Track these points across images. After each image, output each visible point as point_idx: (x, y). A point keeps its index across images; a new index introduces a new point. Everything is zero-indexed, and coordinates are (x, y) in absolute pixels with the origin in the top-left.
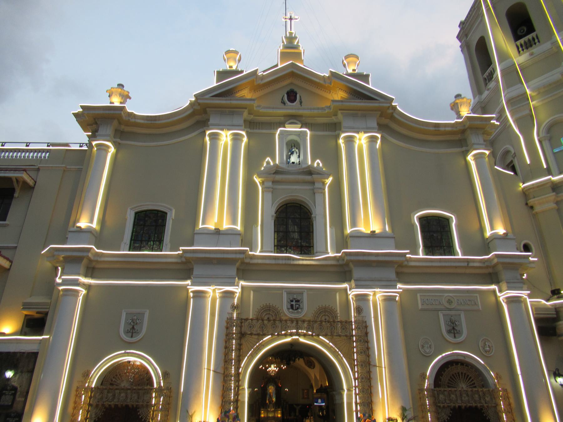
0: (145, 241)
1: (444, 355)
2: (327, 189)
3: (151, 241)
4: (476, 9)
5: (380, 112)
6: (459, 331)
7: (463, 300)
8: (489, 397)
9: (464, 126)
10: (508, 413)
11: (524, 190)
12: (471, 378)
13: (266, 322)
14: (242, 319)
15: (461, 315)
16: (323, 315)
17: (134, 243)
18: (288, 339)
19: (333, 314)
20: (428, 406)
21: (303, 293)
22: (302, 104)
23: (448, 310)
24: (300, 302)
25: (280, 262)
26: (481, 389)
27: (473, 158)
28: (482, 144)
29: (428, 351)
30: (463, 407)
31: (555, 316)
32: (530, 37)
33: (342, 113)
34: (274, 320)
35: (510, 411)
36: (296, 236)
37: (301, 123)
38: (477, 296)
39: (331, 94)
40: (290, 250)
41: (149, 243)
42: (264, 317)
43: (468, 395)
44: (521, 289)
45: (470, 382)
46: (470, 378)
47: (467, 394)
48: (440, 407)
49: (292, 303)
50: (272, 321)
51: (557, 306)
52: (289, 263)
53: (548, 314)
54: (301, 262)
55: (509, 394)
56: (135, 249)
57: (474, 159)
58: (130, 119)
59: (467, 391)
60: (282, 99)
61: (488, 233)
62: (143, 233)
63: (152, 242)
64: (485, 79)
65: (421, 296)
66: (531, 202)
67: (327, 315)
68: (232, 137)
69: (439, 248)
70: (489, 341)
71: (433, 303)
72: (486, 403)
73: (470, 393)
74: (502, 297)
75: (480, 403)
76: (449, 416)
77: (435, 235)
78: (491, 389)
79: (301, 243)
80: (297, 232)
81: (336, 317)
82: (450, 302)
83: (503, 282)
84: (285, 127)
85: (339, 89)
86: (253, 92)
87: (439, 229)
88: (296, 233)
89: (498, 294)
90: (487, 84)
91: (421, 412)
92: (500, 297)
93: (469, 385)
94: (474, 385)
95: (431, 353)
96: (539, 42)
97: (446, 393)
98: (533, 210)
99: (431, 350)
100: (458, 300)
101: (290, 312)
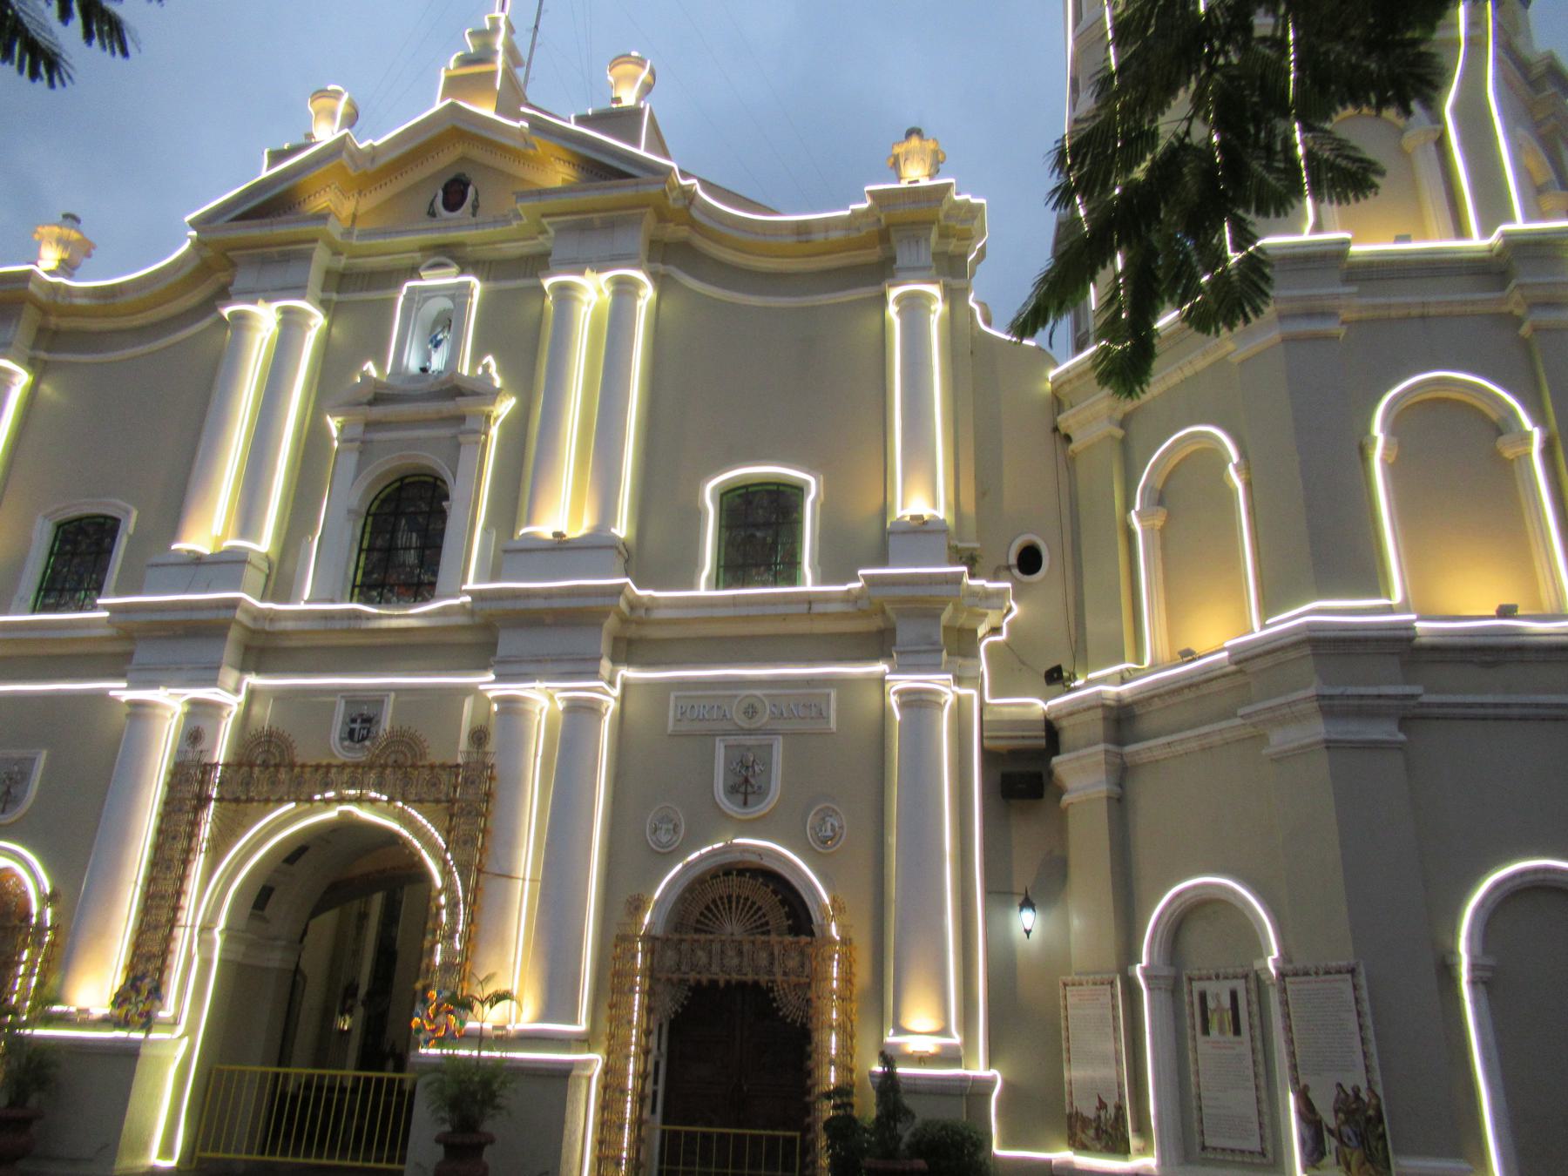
0: (70, 590)
1: (704, 851)
2: (494, 432)
3: (81, 590)
6: (760, 787)
8: (797, 959)
13: (256, 770)
14: (206, 765)
15: (775, 747)
16: (392, 752)
17: (45, 597)
18: (332, 814)
19: (416, 749)
21: (383, 702)
22: (479, 211)
23: (744, 735)
24: (374, 722)
25: (338, 625)
30: (722, 983)
34: (277, 766)
36: (411, 557)
37: (457, 263)
40: (390, 595)
41: (77, 595)
42: (256, 758)
44: (935, 668)
46: (760, 908)
48: (659, 980)
49: (353, 726)
50: (272, 769)
51: (1052, 716)
52: (357, 627)
53: (1016, 738)
54: (385, 624)
56: (46, 608)
58: (59, 299)
59: (740, 942)
60: (432, 204)
62: (69, 571)
63: (83, 593)
65: (677, 697)
66: (1066, 421)
67: (402, 752)
68: (280, 317)
69: (762, 569)
70: (837, 813)
71: (706, 716)
72: (785, 974)
73: (746, 947)
75: (770, 972)
76: (682, 1005)
77: (759, 534)
79: (419, 575)
80: (416, 548)
81: (421, 755)
82: (751, 711)
84: (420, 278)
86: (356, 195)
88: (412, 552)
93: (752, 929)
94: (765, 929)
95: (673, 847)
97: (684, 946)
100: (774, 705)
101: (343, 748)
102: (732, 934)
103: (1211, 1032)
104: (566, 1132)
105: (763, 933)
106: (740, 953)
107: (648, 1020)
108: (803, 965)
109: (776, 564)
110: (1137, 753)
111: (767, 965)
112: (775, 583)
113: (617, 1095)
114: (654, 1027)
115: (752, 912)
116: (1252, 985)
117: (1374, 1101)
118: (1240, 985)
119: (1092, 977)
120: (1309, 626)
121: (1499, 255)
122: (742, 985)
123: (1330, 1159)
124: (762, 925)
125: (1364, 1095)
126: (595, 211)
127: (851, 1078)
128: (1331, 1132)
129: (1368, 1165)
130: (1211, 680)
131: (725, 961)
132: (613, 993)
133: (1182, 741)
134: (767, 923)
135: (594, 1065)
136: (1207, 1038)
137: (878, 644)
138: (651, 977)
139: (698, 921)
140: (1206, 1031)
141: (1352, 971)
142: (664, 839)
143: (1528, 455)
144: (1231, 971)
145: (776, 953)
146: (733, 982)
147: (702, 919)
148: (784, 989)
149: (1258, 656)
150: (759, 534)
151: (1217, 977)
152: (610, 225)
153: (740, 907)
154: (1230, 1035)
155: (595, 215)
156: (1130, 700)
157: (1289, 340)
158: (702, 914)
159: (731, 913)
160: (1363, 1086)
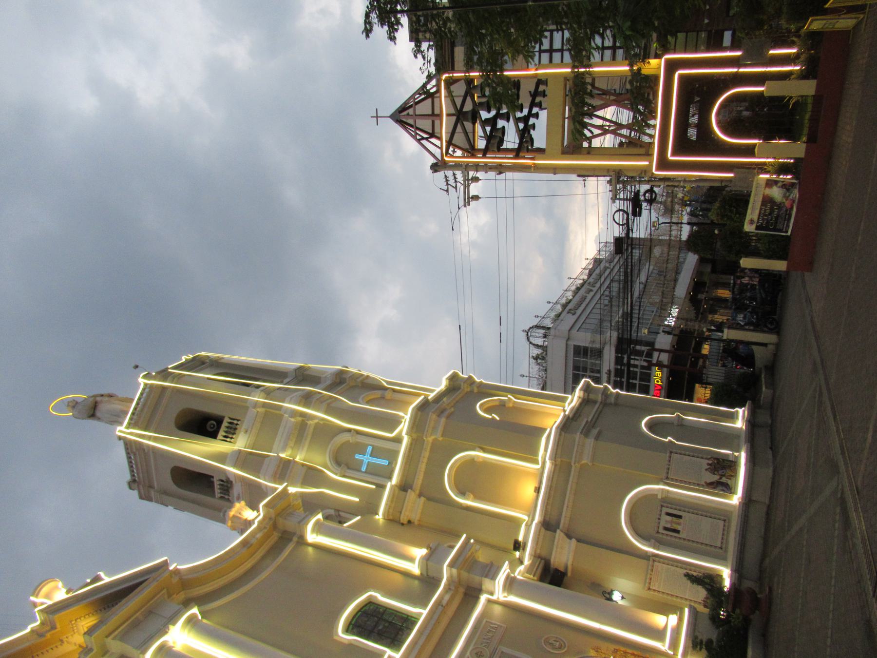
4: (137, 453)
5: (165, 590)
7: (484, 639)
9: (270, 519)
11: (386, 518)
15: (504, 651)
27: (314, 535)
28: (307, 516)
31: (543, 561)
32: (225, 424)
33: (113, 639)
38: (487, 622)
39: (65, 642)
51: (533, 553)
53: (538, 566)
57: (317, 535)
61: (415, 569)
64: (221, 497)
66: (404, 519)
69: (400, 633)
74: (500, 595)
77: (380, 628)
83: (483, 582)
85: (76, 620)
87: (376, 619)
89: (494, 598)
90: (228, 499)
92: (498, 598)
96: (238, 420)
98: (414, 523)
100: (482, 644)
103: (679, 529)
109: (402, 626)
110: (564, 523)
112: (411, 630)
116: (665, 504)
117: (712, 459)
118: (665, 510)
119: (649, 571)
120: (557, 428)
121: (450, 384)
123: (729, 482)
125: (710, 462)
126: (136, 612)
128: (721, 478)
129: (732, 469)
130: (553, 478)
133: (569, 500)
136: (681, 533)
137: (471, 594)
140: (678, 532)
141: (671, 452)
143: (514, 401)
144: (658, 512)
149: (557, 449)
150: (380, 628)
151: (659, 519)
152: (150, 613)
154: (681, 521)
155: (137, 614)
156: (543, 518)
157: (448, 417)
160: (707, 461)
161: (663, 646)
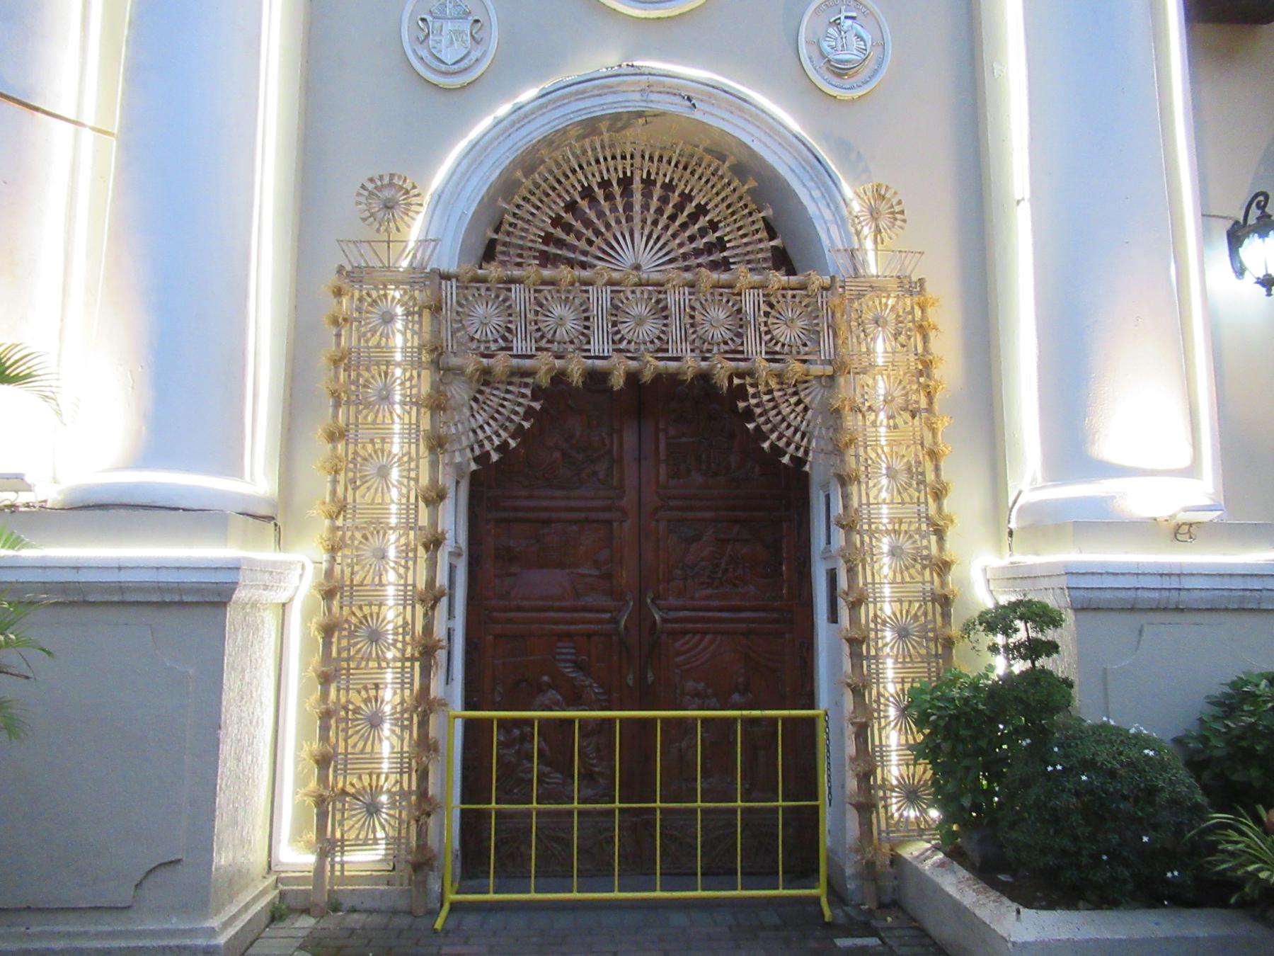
10: (907, 416)
12: (706, 213)
20: (398, 372)
26: (756, 278)
29: (449, 56)
30: (618, 381)
35: (923, 403)
43: (665, 308)
45: (692, 239)
46: (701, 210)
47: (658, 302)
48: (459, 371)
55: (930, 311)
59: (662, 285)
70: (869, 13)
72: (772, 357)
75: (736, 354)
76: (518, 432)
78: (817, 280)
91: (331, 402)
93: (685, 257)
94: (716, 256)
97: (517, 293)
99: (474, 55)
102: (637, 267)
104: (226, 749)
105: (714, 266)
106: (661, 311)
107: (434, 465)
108: (813, 333)
111: (728, 335)
113: (363, 645)
114: (446, 479)
115: (682, 218)
122: (668, 383)
124: (709, 248)
127: (943, 584)
131: (624, 329)
132: (337, 405)
134: (721, 244)
135: (293, 577)
138: (436, 365)
139: (548, 239)
142: (449, 56)
145: (749, 308)
146: (647, 376)
147: (559, 233)
148: (770, 392)
153: (654, 204)
158: (557, 221)
159: (629, 219)
161: (1034, 480)
